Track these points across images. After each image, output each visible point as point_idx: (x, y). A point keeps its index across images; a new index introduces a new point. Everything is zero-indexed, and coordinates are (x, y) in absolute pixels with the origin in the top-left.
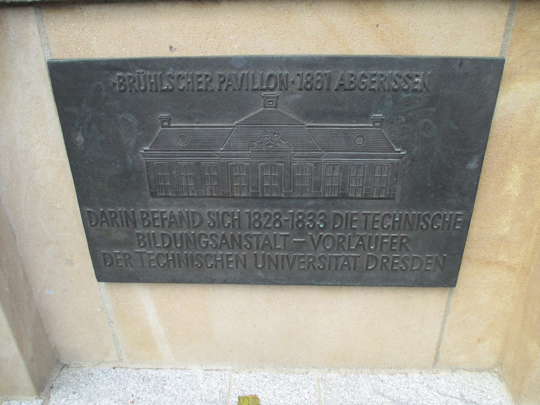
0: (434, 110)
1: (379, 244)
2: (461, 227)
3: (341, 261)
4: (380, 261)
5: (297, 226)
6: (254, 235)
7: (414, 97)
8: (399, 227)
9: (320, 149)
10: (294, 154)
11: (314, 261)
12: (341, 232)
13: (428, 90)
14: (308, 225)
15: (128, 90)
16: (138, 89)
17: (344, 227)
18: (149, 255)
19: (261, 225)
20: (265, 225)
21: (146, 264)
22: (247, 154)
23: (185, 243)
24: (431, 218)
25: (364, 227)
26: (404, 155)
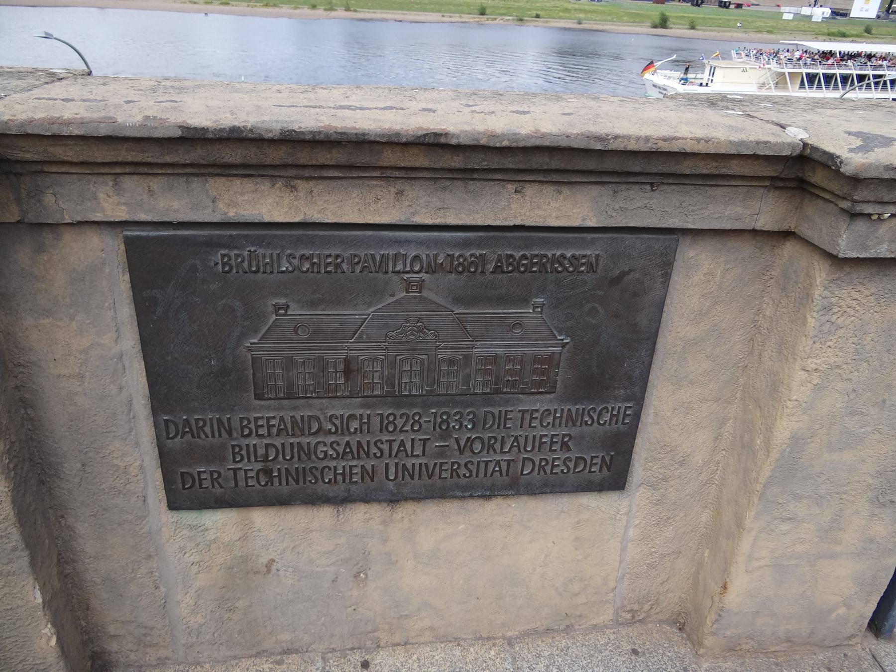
1: (537, 444)
2: (630, 421)
3: (491, 466)
4: (537, 463)
5: (440, 428)
6: (387, 441)
8: (560, 423)
9: (471, 339)
11: (458, 468)
14: (454, 427)
15: (234, 271)
16: (247, 270)
17: (496, 426)
18: (246, 471)
19: (395, 428)
20: (403, 427)
21: (242, 483)
23: (296, 455)
24: (597, 413)
26: (567, 343)
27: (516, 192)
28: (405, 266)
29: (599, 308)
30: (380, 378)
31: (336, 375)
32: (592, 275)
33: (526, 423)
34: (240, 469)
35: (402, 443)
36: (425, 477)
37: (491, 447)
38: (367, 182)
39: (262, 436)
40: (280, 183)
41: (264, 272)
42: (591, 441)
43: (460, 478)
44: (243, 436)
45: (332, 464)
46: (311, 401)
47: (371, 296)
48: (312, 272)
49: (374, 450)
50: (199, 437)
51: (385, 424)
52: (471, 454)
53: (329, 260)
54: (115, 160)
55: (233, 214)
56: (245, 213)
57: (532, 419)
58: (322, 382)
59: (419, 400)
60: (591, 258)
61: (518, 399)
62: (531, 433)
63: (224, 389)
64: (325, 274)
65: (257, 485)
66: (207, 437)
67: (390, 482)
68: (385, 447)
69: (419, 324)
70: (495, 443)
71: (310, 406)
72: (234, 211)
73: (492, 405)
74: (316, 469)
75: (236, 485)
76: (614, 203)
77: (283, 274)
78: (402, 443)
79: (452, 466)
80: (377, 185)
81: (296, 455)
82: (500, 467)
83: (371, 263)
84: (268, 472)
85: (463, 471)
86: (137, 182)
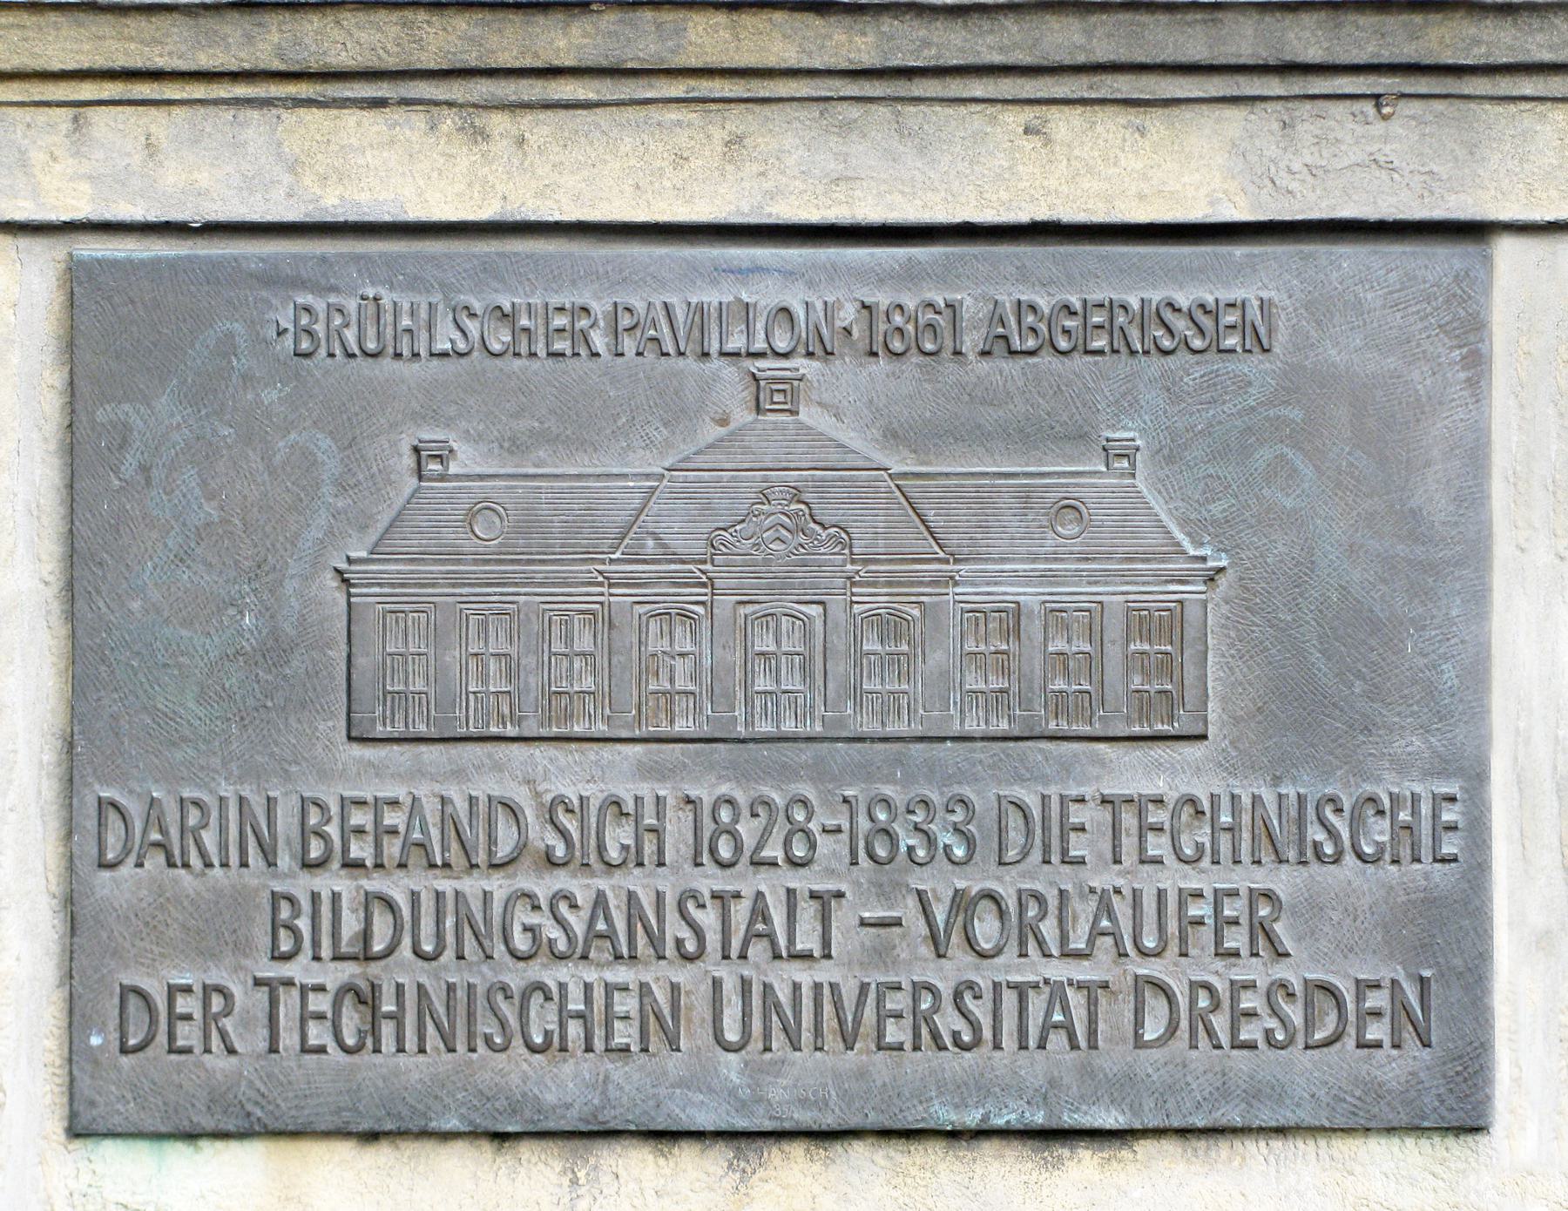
0: (1296, 414)
1: (1172, 926)
4: (1183, 1002)
5: (872, 856)
7: (1228, 373)
9: (942, 555)
10: (857, 572)
12: (1032, 876)
13: (1268, 351)
14: (911, 849)
15: (323, 352)
16: (357, 351)
17: (1036, 855)
19: (738, 848)
21: (289, 1040)
22: (699, 574)
23: (450, 939)
25: (1109, 856)
26: (1221, 570)
27: (1027, 131)
28: (749, 333)
29: (1298, 463)
30: (694, 678)
31: (571, 663)
32: (1261, 362)
33: (1129, 844)
34: (289, 983)
35: (760, 912)
36: (832, 1041)
37: (1027, 934)
38: (654, 113)
39: (358, 865)
40: (449, 122)
41: (398, 355)
42: (1348, 921)
43: (946, 1049)
44: (307, 865)
45: (552, 976)
46: (501, 750)
47: (666, 425)
48: (517, 355)
49: (675, 928)
50: (186, 865)
51: (707, 835)
52: (971, 958)
53: (560, 321)
54: (86, 66)
55: (336, 202)
56: (364, 197)
57: (1144, 829)
58: (533, 685)
59: (807, 753)
60: (1249, 310)
61: (1101, 762)
62: (1148, 882)
63: (270, 704)
64: (550, 361)
65: (332, 1047)
66: (208, 865)
67: (732, 1056)
68: (708, 918)
69: (793, 507)
70: (1043, 916)
71: (498, 767)
72: (338, 193)
73: (1020, 780)
74: (504, 988)
75: (273, 1049)
76: (1289, 155)
77: (445, 361)
78: (760, 912)
79: (916, 1000)
80: (679, 123)
81: (450, 939)
82: (1066, 1010)
83: (666, 330)
84: (366, 998)
85: (949, 1021)
86: (124, 122)
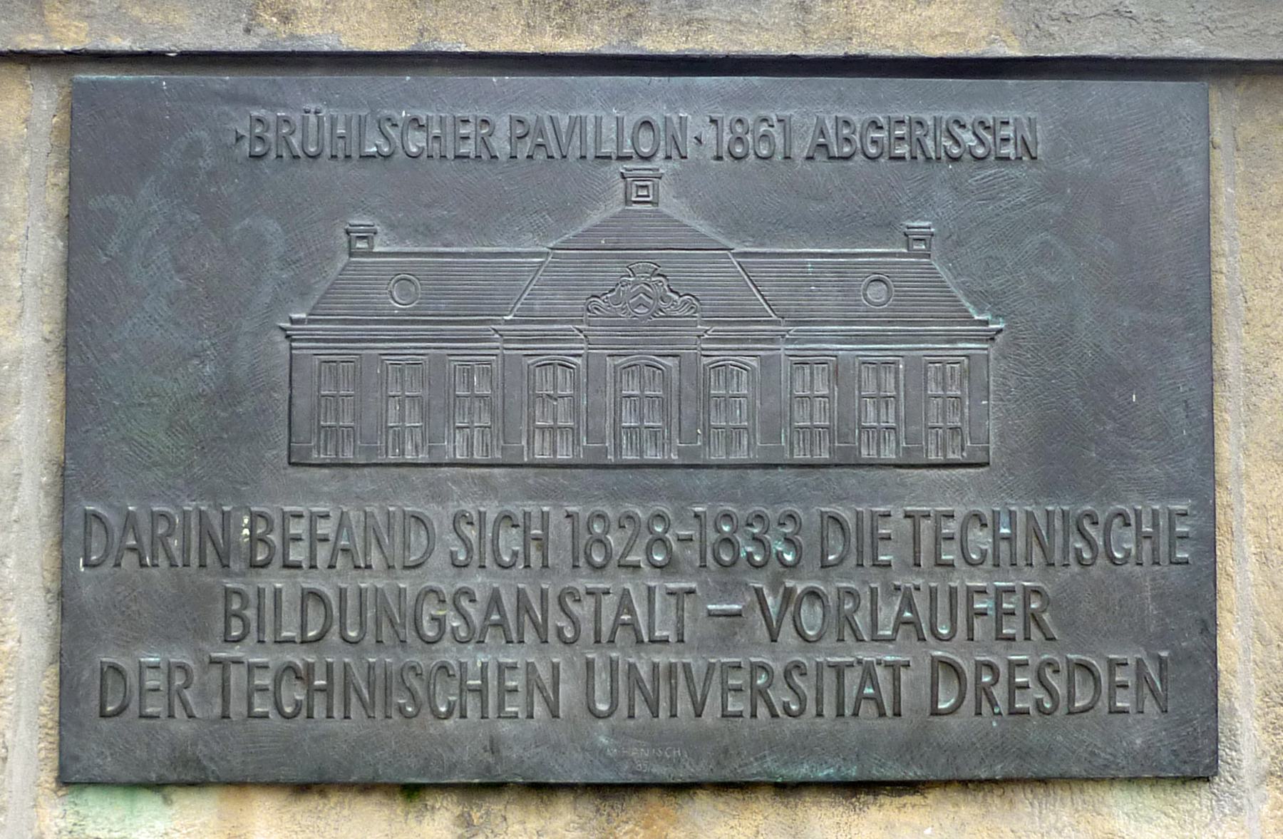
0: (1056, 208)
6: (590, 593)
7: (1003, 176)
9: (775, 318)
10: (706, 331)
12: (848, 577)
13: (1035, 158)
14: (750, 555)
15: (273, 155)
16: (300, 153)
17: (852, 560)
18: (251, 668)
19: (608, 556)
21: (237, 708)
22: (576, 332)
23: (370, 624)
25: (911, 561)
26: (999, 331)
31: (472, 403)
34: (238, 662)
35: (625, 603)
49: (557, 620)
51: (582, 543)
57: (939, 538)
63: (225, 436)
65: (273, 715)
67: (601, 723)
68: (583, 611)
81: (370, 624)
82: (875, 686)
85: (781, 696)
